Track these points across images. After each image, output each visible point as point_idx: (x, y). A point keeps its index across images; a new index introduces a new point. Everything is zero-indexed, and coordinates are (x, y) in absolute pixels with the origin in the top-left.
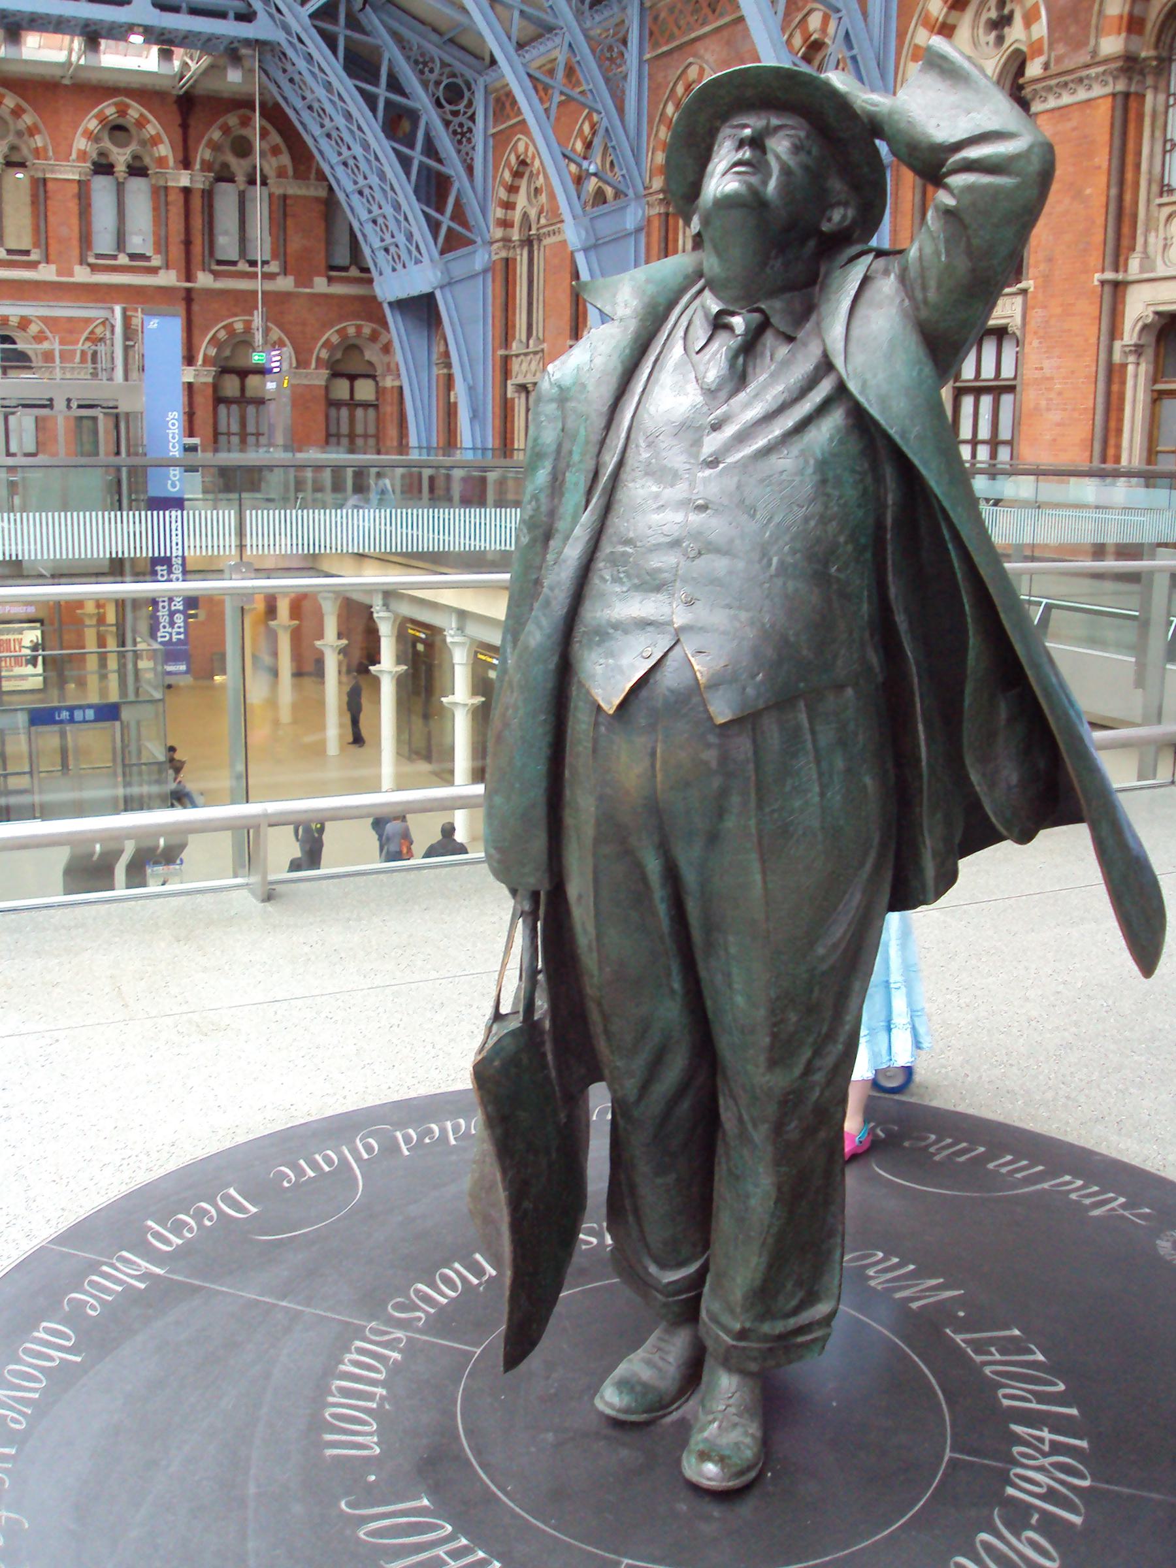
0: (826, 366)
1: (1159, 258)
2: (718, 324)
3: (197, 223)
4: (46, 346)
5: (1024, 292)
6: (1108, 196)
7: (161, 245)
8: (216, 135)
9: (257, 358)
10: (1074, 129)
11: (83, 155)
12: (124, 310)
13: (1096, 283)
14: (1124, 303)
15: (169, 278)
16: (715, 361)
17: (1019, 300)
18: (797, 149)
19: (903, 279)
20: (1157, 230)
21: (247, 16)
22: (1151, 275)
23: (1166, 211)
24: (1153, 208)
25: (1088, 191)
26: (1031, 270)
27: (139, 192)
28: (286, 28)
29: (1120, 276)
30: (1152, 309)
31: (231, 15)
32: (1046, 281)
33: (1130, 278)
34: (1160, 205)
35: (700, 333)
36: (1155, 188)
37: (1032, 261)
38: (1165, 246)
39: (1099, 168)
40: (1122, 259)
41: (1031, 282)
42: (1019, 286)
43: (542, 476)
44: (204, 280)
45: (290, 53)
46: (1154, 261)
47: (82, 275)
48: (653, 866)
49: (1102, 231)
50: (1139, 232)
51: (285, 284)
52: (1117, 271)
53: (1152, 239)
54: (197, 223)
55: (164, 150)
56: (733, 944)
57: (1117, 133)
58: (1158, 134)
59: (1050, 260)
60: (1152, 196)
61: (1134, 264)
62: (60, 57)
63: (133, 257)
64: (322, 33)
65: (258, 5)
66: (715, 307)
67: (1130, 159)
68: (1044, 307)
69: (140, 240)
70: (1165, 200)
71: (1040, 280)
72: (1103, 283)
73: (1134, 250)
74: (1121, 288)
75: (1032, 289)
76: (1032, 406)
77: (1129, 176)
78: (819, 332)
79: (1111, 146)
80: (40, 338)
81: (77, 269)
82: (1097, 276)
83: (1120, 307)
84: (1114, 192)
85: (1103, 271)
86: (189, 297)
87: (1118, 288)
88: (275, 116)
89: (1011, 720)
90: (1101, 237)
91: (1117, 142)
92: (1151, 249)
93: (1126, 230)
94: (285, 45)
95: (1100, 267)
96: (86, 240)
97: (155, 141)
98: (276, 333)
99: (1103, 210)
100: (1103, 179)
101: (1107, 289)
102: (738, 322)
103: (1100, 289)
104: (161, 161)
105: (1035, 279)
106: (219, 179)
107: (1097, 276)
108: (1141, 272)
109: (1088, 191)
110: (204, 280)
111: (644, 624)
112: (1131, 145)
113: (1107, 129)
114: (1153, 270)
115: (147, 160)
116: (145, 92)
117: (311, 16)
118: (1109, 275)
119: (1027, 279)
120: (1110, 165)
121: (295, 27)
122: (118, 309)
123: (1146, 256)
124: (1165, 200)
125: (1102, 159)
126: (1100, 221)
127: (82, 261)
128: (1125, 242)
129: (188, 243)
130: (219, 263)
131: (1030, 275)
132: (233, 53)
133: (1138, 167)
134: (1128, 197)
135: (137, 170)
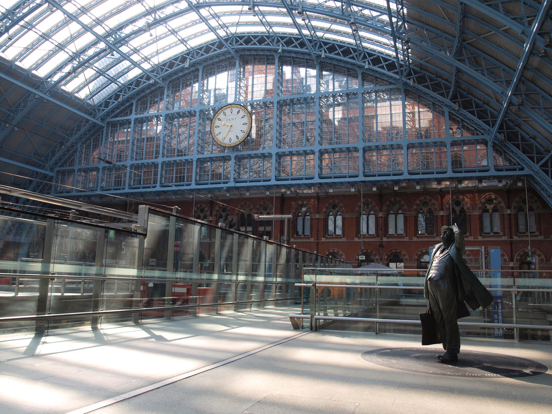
3: (513, 222)
4: (471, 257)
7: (503, 229)
8: (518, 199)
9: (529, 259)
11: (480, 208)
12: (485, 248)
15: (505, 238)
21: (522, 169)
27: (497, 216)
28: (533, 171)
31: (518, 169)
44: (515, 238)
45: (535, 177)
47: (480, 238)
51: (541, 238)
54: (513, 222)
55: (503, 204)
62: (474, 185)
63: (494, 233)
64: (543, 170)
65: (525, 166)
69: (497, 228)
80: (469, 255)
81: (479, 237)
86: (511, 243)
88: (533, 192)
94: (533, 175)
96: (482, 229)
97: (500, 203)
98: (538, 252)
104: (502, 207)
106: (519, 211)
110: (515, 238)
115: (498, 208)
116: (497, 191)
117: (540, 167)
121: (535, 170)
122: (483, 247)
127: (481, 235)
129: (510, 228)
130: (520, 233)
132: (519, 178)
135: (495, 210)
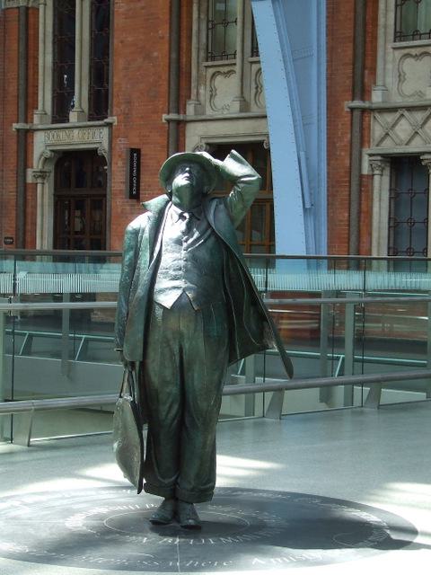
0: (209, 225)
1: (208, 104)
2: (181, 217)
5: (110, 125)
6: (170, 58)
10: (143, 8)
13: (164, 121)
14: (184, 135)
16: (182, 225)
17: (105, 131)
18: (198, 172)
19: (226, 206)
20: (205, 85)
22: (203, 117)
23: (211, 71)
24: (202, 68)
25: (155, 54)
26: (115, 108)
29: (181, 117)
30: (205, 141)
32: (126, 117)
33: (188, 118)
34: (206, 67)
35: (176, 217)
36: (202, 54)
37: (115, 103)
38: (211, 96)
39: (163, 38)
40: (181, 106)
41: (115, 118)
42: (106, 120)
43: (131, 253)
46: (204, 107)
48: (176, 349)
49: (166, 83)
50: (193, 85)
52: (178, 112)
53: (202, 91)
56: (196, 367)
57: (175, 14)
58: (202, 16)
59: (129, 102)
60: (200, 61)
61: (190, 109)
66: (180, 211)
67: (184, 34)
68: (126, 137)
70: (210, 63)
71: (122, 117)
72: (169, 121)
73: (189, 97)
74: (181, 125)
75: (116, 123)
76: (119, 210)
77: (184, 45)
78: (206, 217)
79: (170, 24)
82: (165, 116)
83: (182, 139)
84: (174, 56)
85: (168, 114)
87: (180, 125)
89: (254, 313)
90: (164, 88)
91: (175, 19)
92: (202, 98)
93: (183, 84)
95: (166, 109)
99: (167, 69)
100: (167, 46)
101: (172, 126)
102: (186, 215)
103: (167, 125)
105: (118, 116)
107: (165, 116)
108: (195, 114)
109: (155, 54)
111: (175, 288)
112: (184, 24)
113: (167, 10)
114: (203, 113)
118: (173, 116)
119: (112, 116)
120: (170, 37)
123: (199, 103)
124: (210, 63)
125: (164, 31)
126: (165, 76)
128: (183, 93)
131: (114, 113)
133: (190, 38)
134: (184, 60)
